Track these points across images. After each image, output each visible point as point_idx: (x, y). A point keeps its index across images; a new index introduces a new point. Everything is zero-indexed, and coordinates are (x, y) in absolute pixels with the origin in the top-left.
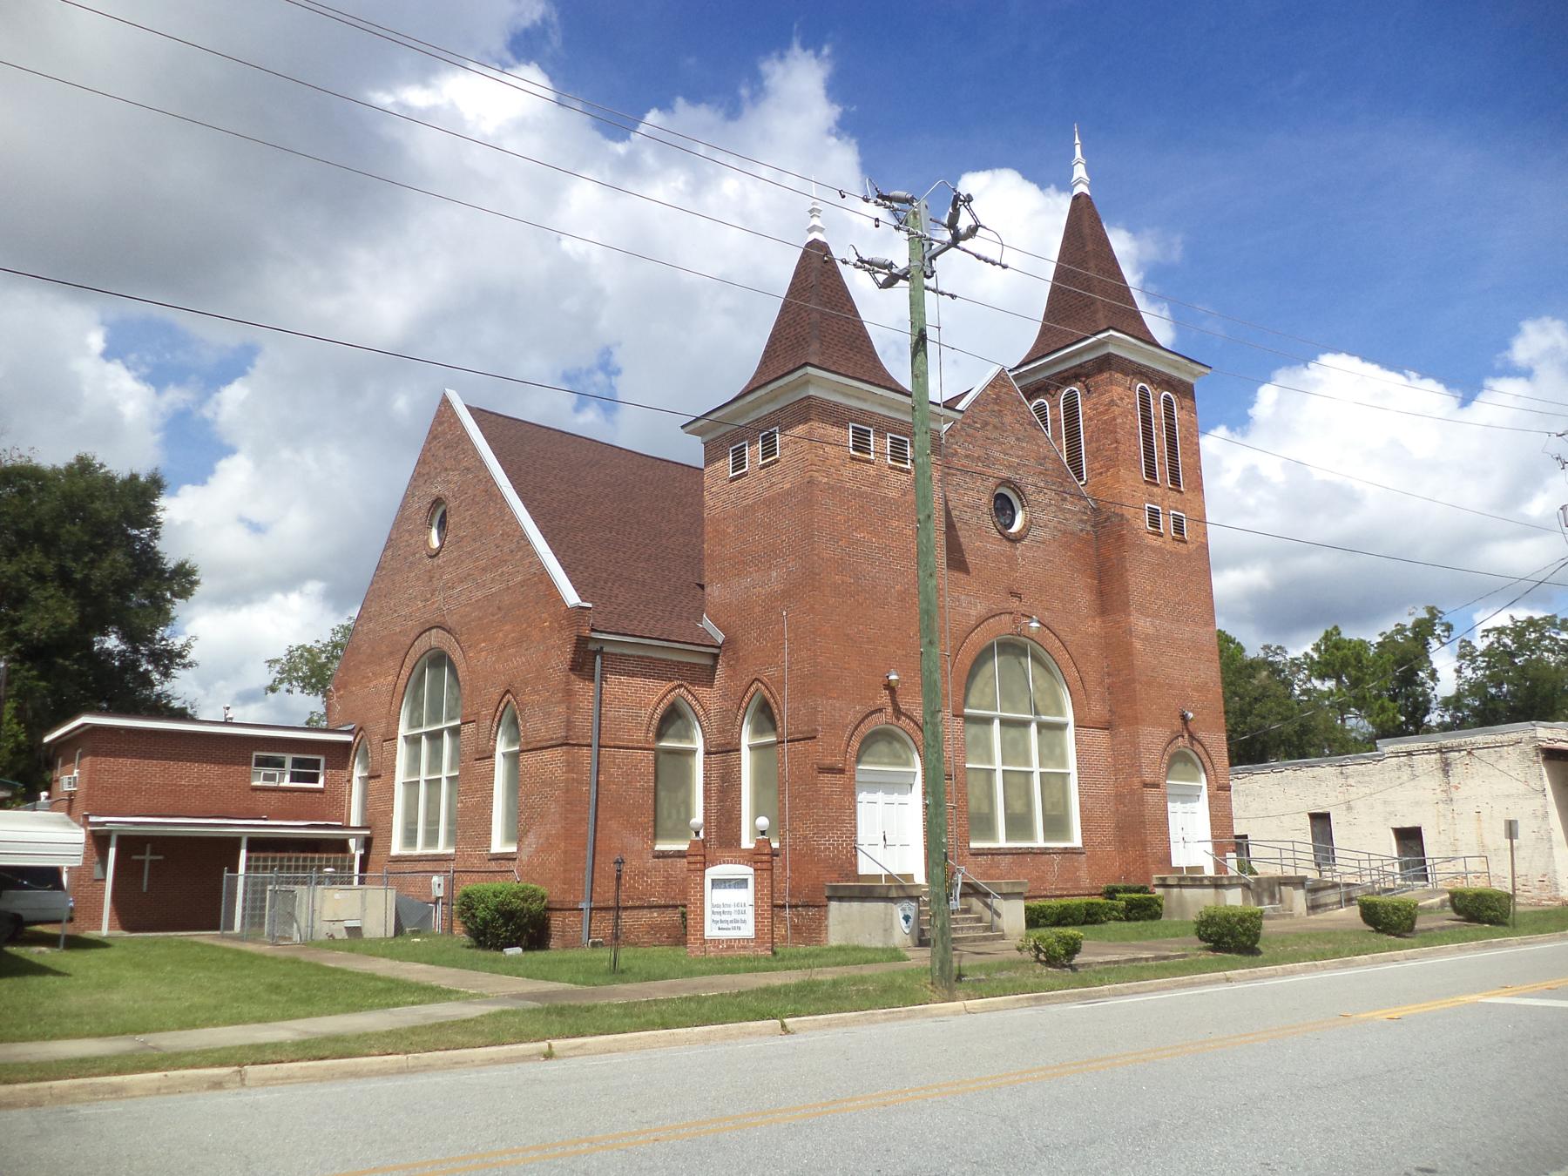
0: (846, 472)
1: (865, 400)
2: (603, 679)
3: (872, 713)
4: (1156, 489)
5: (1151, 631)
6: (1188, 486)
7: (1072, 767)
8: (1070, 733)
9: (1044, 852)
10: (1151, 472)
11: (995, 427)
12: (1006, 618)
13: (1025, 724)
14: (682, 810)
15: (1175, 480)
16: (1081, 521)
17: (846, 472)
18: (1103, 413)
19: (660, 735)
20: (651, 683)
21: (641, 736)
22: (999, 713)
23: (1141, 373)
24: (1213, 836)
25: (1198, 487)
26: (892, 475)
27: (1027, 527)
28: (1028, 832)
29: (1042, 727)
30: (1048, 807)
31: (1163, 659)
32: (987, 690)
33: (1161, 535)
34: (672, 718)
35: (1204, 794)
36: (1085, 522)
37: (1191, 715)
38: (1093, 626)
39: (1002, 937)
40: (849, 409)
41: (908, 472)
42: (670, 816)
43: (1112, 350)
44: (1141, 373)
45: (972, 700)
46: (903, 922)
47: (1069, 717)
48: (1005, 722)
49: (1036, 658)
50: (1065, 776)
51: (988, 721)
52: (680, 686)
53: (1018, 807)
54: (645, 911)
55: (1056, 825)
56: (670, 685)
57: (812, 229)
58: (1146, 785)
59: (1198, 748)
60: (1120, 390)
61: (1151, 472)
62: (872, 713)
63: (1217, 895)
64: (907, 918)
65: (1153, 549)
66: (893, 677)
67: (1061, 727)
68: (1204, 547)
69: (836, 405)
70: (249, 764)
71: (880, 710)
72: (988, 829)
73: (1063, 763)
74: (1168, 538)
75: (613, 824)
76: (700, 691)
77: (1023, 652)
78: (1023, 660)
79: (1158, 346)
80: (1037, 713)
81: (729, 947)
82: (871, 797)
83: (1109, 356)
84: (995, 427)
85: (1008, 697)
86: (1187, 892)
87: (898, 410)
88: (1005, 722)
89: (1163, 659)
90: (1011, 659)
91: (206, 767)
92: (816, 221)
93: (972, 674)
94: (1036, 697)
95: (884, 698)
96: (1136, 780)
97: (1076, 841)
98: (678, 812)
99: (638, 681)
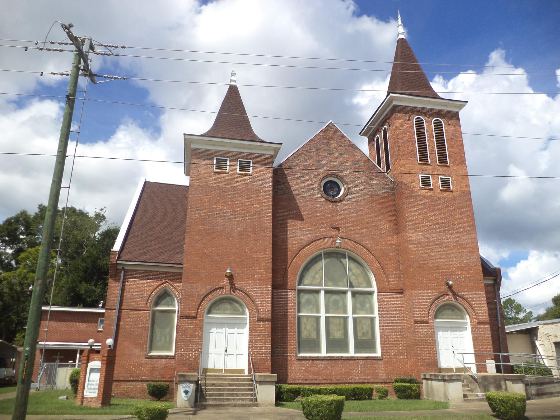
0: (211, 179)
1: (225, 146)
2: (124, 280)
3: (216, 289)
4: (427, 167)
5: (423, 239)
6: (454, 163)
7: (376, 314)
8: (375, 295)
9: (352, 359)
10: (424, 158)
11: (325, 150)
12: (329, 240)
13: (345, 293)
14: (168, 337)
15: (443, 160)
16: (384, 188)
17: (211, 179)
18: (394, 134)
19: (157, 304)
20: (150, 282)
21: (143, 304)
22: (324, 287)
23: (417, 111)
24: (475, 351)
25: (463, 162)
26: (240, 178)
27: (345, 196)
28: (344, 347)
29: (354, 294)
30: (360, 334)
31: (433, 254)
32: (317, 276)
33: (432, 189)
34: (164, 296)
35: (469, 326)
36: (387, 189)
37: (451, 283)
38: (391, 240)
39: (257, 405)
40: (215, 151)
41: (228, 173)
42: (160, 340)
43: (395, 103)
44: (417, 111)
45: (306, 281)
46: (184, 395)
47: (375, 288)
48: (327, 292)
49: (350, 258)
50: (372, 319)
51: (318, 292)
52: (166, 282)
53: (338, 335)
54: (140, 383)
55: (365, 344)
56: (161, 282)
57: (231, 81)
58: (416, 322)
59: (460, 300)
60: (401, 121)
61: (424, 158)
62: (216, 289)
63: (445, 385)
64: (186, 392)
65: (424, 197)
66: (228, 271)
67: (371, 293)
68: (468, 193)
69: (207, 150)
70: (97, 323)
71: (222, 288)
72: (316, 346)
73: (372, 312)
74: (437, 190)
75: (126, 344)
76: (177, 284)
77: (344, 256)
78: (343, 260)
79: (439, 98)
80: (351, 286)
81: (91, 401)
82: (219, 330)
83: (395, 106)
84: (325, 150)
85: (330, 278)
86: (435, 384)
87: (245, 148)
88: (327, 292)
89: (433, 254)
90: (335, 260)
91: (81, 324)
92: (233, 78)
93: (307, 268)
94: (353, 279)
95: (226, 281)
96: (412, 320)
97: (379, 354)
98: (165, 338)
99: (144, 281)
